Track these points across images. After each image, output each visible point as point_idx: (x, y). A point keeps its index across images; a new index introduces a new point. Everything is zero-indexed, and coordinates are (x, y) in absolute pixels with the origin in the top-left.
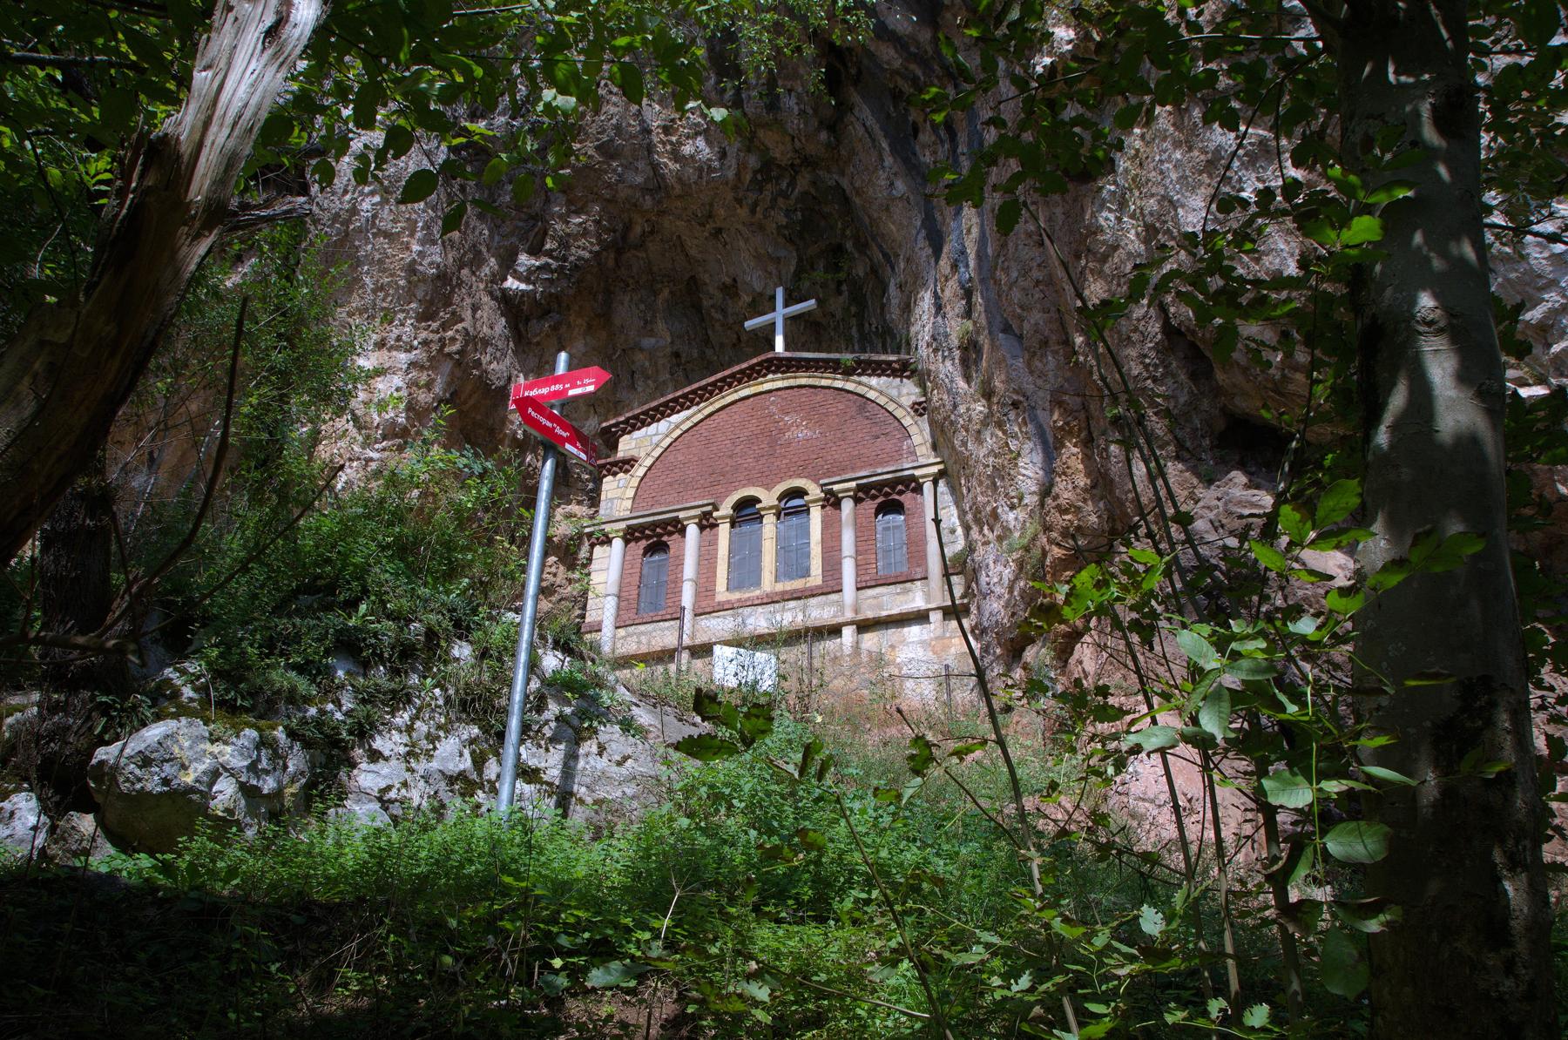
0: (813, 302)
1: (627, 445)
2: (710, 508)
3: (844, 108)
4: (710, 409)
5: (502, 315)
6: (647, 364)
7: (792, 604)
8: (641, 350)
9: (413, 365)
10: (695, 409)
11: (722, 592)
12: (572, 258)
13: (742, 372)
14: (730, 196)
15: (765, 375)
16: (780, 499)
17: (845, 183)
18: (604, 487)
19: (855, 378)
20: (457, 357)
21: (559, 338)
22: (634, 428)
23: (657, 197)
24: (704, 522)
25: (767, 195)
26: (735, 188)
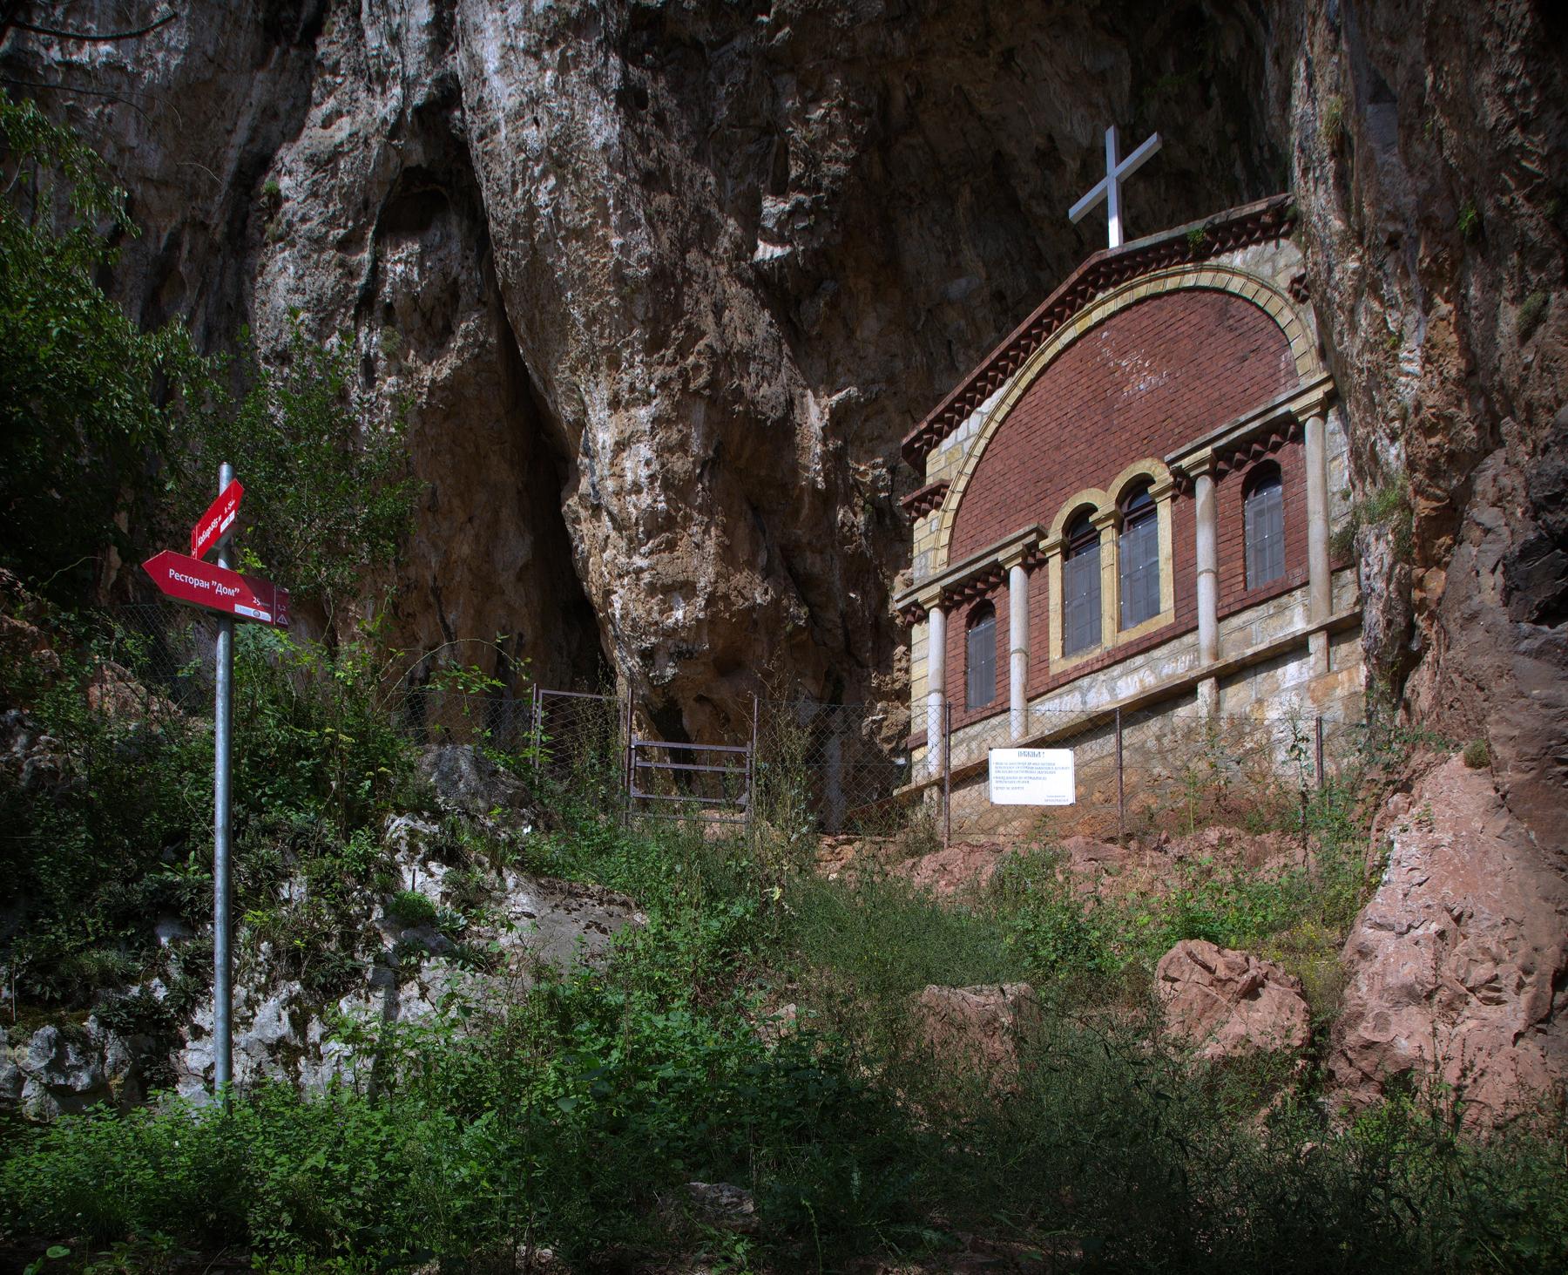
2: (1033, 537)
4: (1030, 376)
5: (763, 306)
9: (657, 421)
10: (1009, 382)
11: (1058, 663)
16: (1119, 502)
20: (707, 392)
24: (1031, 560)
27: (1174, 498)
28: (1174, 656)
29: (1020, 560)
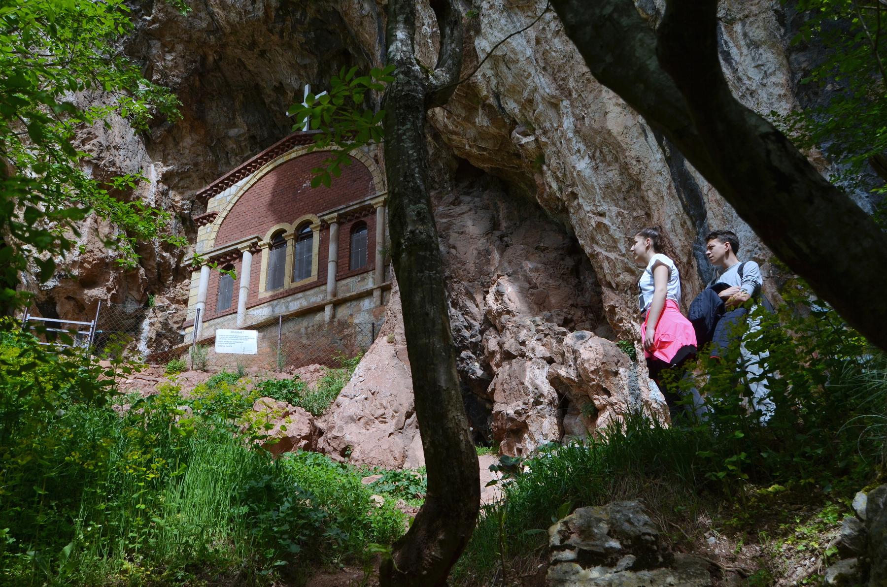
1: (213, 204)
2: (256, 240)
4: (261, 174)
6: (234, 146)
8: (229, 138)
10: (251, 175)
13: (278, 147)
14: (264, 28)
15: (292, 148)
16: (297, 229)
17: (339, 8)
18: (199, 233)
21: (174, 139)
22: (217, 192)
23: (218, 35)
24: (253, 249)
26: (266, 22)
27: (321, 231)
28: (316, 294)
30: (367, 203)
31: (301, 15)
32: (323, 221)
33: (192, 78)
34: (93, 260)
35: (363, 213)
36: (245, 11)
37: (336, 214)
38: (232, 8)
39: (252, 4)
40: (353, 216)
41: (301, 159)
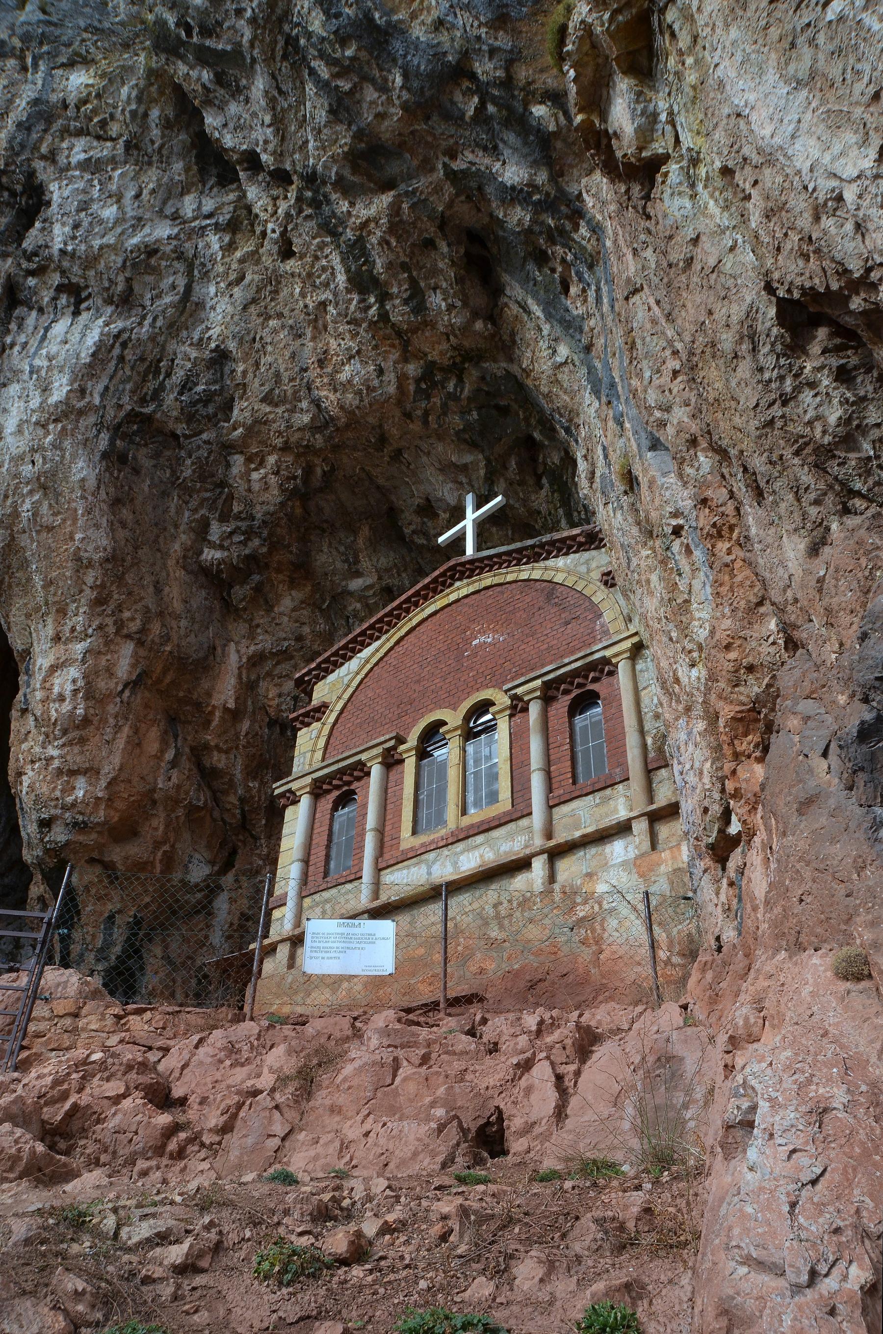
0: (499, 498)
1: (321, 692)
2: (392, 743)
3: (496, 291)
7: (480, 839)
8: (351, 594)
10: (384, 638)
11: (407, 839)
12: (259, 516)
13: (426, 587)
14: (397, 413)
15: (451, 585)
16: (467, 719)
19: (542, 564)
21: (266, 602)
23: (327, 432)
24: (391, 761)
25: (437, 400)
26: (399, 403)
27: (511, 716)
29: (380, 760)
30: (597, 656)
31: (456, 386)
32: (515, 698)
33: (290, 503)
34: (130, 795)
35: (592, 675)
36: (368, 388)
37: (539, 682)
38: (348, 386)
39: (378, 377)
40: (572, 683)
41: (466, 601)
